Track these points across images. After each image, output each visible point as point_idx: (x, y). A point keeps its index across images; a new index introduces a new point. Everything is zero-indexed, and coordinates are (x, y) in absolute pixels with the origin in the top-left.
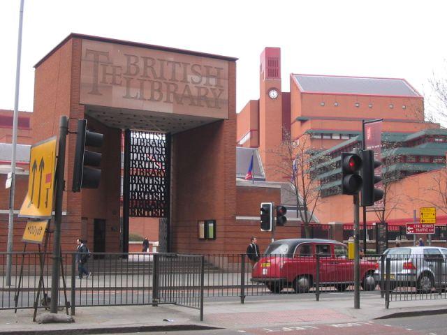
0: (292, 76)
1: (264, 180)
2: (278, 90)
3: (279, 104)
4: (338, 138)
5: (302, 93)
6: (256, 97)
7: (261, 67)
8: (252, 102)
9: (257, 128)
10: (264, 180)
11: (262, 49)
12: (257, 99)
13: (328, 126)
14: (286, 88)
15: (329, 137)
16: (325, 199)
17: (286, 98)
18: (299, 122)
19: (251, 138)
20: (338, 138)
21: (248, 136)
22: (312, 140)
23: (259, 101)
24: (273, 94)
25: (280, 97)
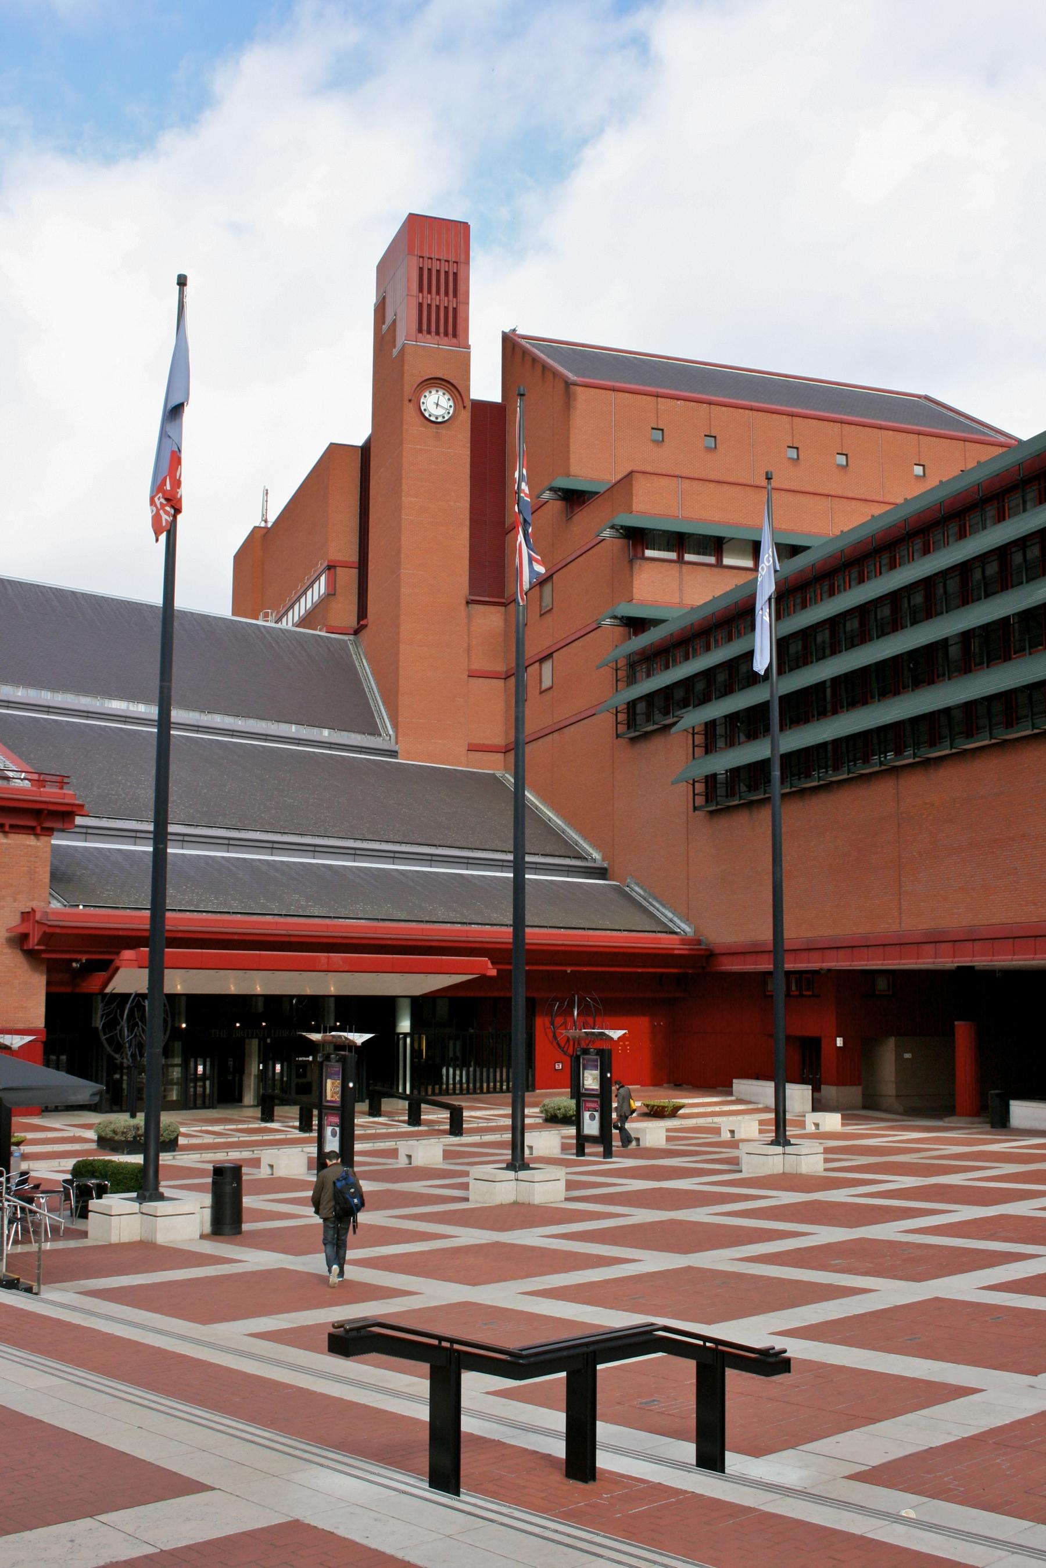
0: (513, 347)
1: (394, 754)
2: (455, 386)
6: (357, 431)
7: (380, 310)
8: (334, 449)
9: (355, 558)
10: (394, 754)
12: (359, 441)
16: (723, 823)
17: (488, 424)
18: (559, 504)
19: (331, 593)
21: (320, 587)
23: (365, 451)
24: (437, 404)
25: (466, 416)
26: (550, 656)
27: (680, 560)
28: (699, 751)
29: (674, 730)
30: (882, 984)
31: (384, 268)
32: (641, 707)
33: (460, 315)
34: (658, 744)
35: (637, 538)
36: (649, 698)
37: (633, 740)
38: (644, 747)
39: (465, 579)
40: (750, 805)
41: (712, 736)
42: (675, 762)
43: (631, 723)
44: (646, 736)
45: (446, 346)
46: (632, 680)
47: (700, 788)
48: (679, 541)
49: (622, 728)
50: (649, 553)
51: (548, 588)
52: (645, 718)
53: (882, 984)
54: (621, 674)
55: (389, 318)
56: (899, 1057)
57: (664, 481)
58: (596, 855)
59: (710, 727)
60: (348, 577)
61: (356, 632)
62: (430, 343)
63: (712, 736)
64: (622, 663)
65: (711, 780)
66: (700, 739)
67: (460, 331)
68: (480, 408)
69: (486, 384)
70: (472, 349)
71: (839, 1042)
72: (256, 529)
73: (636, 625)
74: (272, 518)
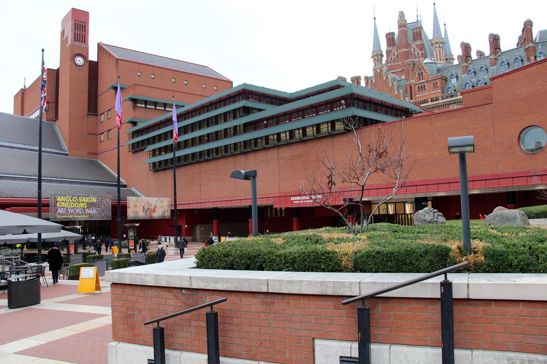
0: (100, 47)
2: (85, 57)
3: (85, 73)
4: (163, 108)
5: (117, 60)
7: (63, 33)
9: (54, 100)
11: (67, 10)
12: (56, 69)
13: (152, 96)
14: (93, 56)
15: (153, 107)
17: (93, 67)
20: (163, 108)
22: (135, 107)
23: (58, 71)
24: (80, 61)
25: (87, 64)
26: (110, 130)
27: (146, 107)
28: (151, 156)
29: (145, 151)
30: (196, 212)
31: (64, 21)
32: (136, 145)
33: (86, 37)
34: (140, 154)
35: (135, 101)
36: (138, 142)
37: (134, 153)
38: (136, 154)
39: (86, 108)
40: (164, 169)
41: (154, 153)
42: (145, 160)
43: (133, 148)
44: (137, 152)
45: (82, 45)
46: (133, 138)
47: (151, 165)
48: (146, 102)
49: (131, 150)
50: (138, 105)
51: (110, 112)
52: (137, 148)
53: (196, 212)
54: (131, 136)
55: (66, 36)
56: (200, 229)
57: (142, 87)
58: (124, 182)
59: (154, 151)
60: (53, 106)
61: (55, 121)
62: (77, 44)
63: (154, 153)
64: (131, 133)
65: (154, 164)
66: (151, 153)
67: (86, 41)
68: (91, 63)
69: (93, 56)
70: (90, 47)
71: (186, 226)
72: (22, 89)
73: (134, 124)
74: (27, 86)
